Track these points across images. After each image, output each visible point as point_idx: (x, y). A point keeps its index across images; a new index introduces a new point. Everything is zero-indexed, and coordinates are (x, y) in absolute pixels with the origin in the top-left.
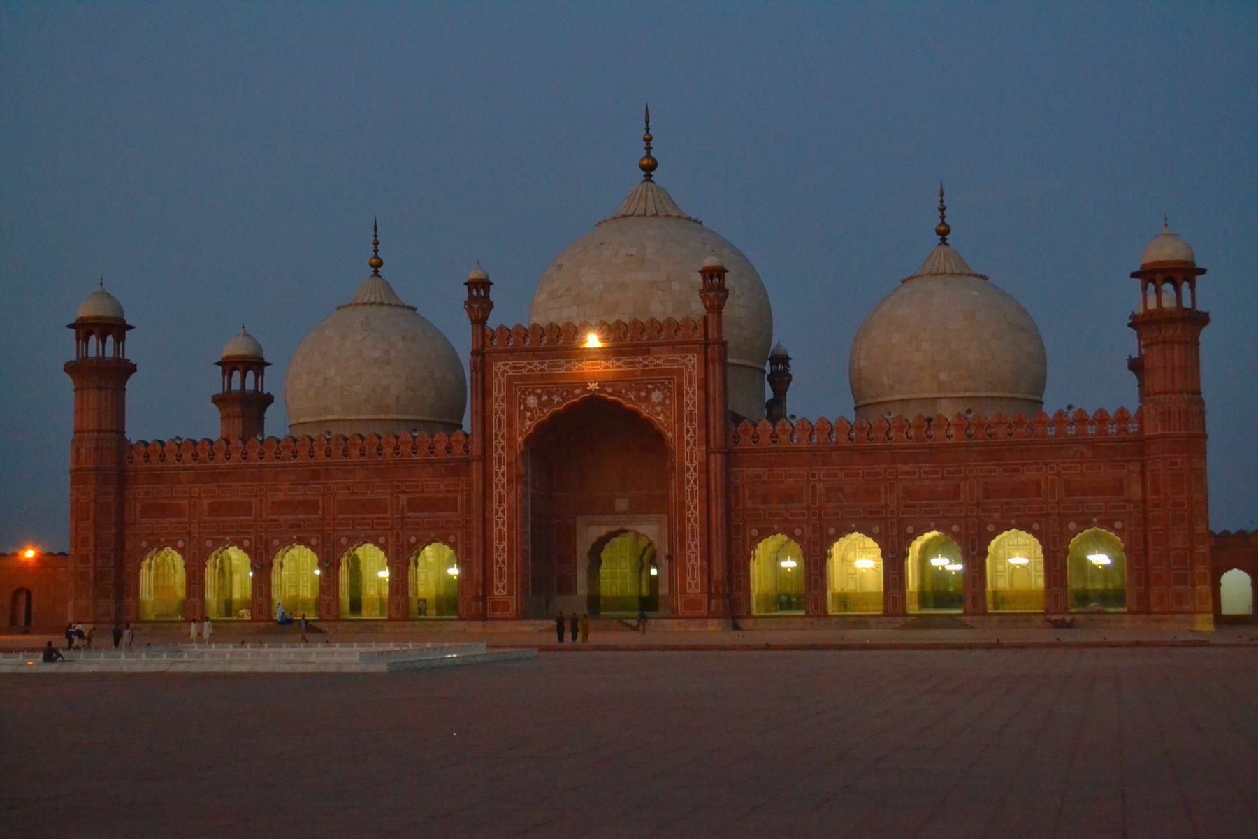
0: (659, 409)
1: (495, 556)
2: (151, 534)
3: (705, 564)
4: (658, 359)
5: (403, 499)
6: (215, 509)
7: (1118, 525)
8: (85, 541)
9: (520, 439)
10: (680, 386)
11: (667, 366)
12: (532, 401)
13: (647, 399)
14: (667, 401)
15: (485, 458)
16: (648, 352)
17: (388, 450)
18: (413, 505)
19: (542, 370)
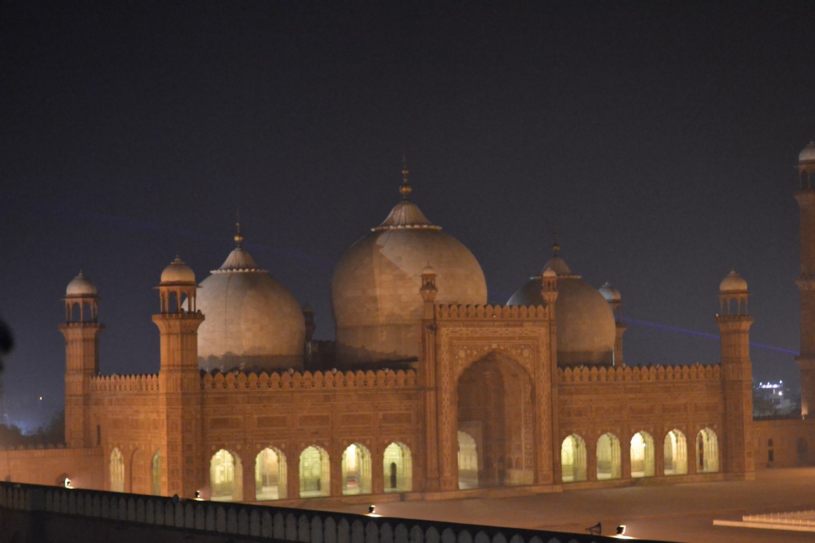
0: (527, 361)
1: (445, 450)
2: (219, 440)
3: (551, 453)
4: (526, 330)
5: (381, 414)
6: (261, 422)
7: (715, 426)
8: (190, 446)
9: (456, 378)
10: (538, 346)
11: (531, 335)
12: (462, 354)
13: (521, 354)
14: (531, 356)
15: (437, 389)
16: (521, 325)
17: (371, 382)
18: (385, 418)
19: (467, 334)
